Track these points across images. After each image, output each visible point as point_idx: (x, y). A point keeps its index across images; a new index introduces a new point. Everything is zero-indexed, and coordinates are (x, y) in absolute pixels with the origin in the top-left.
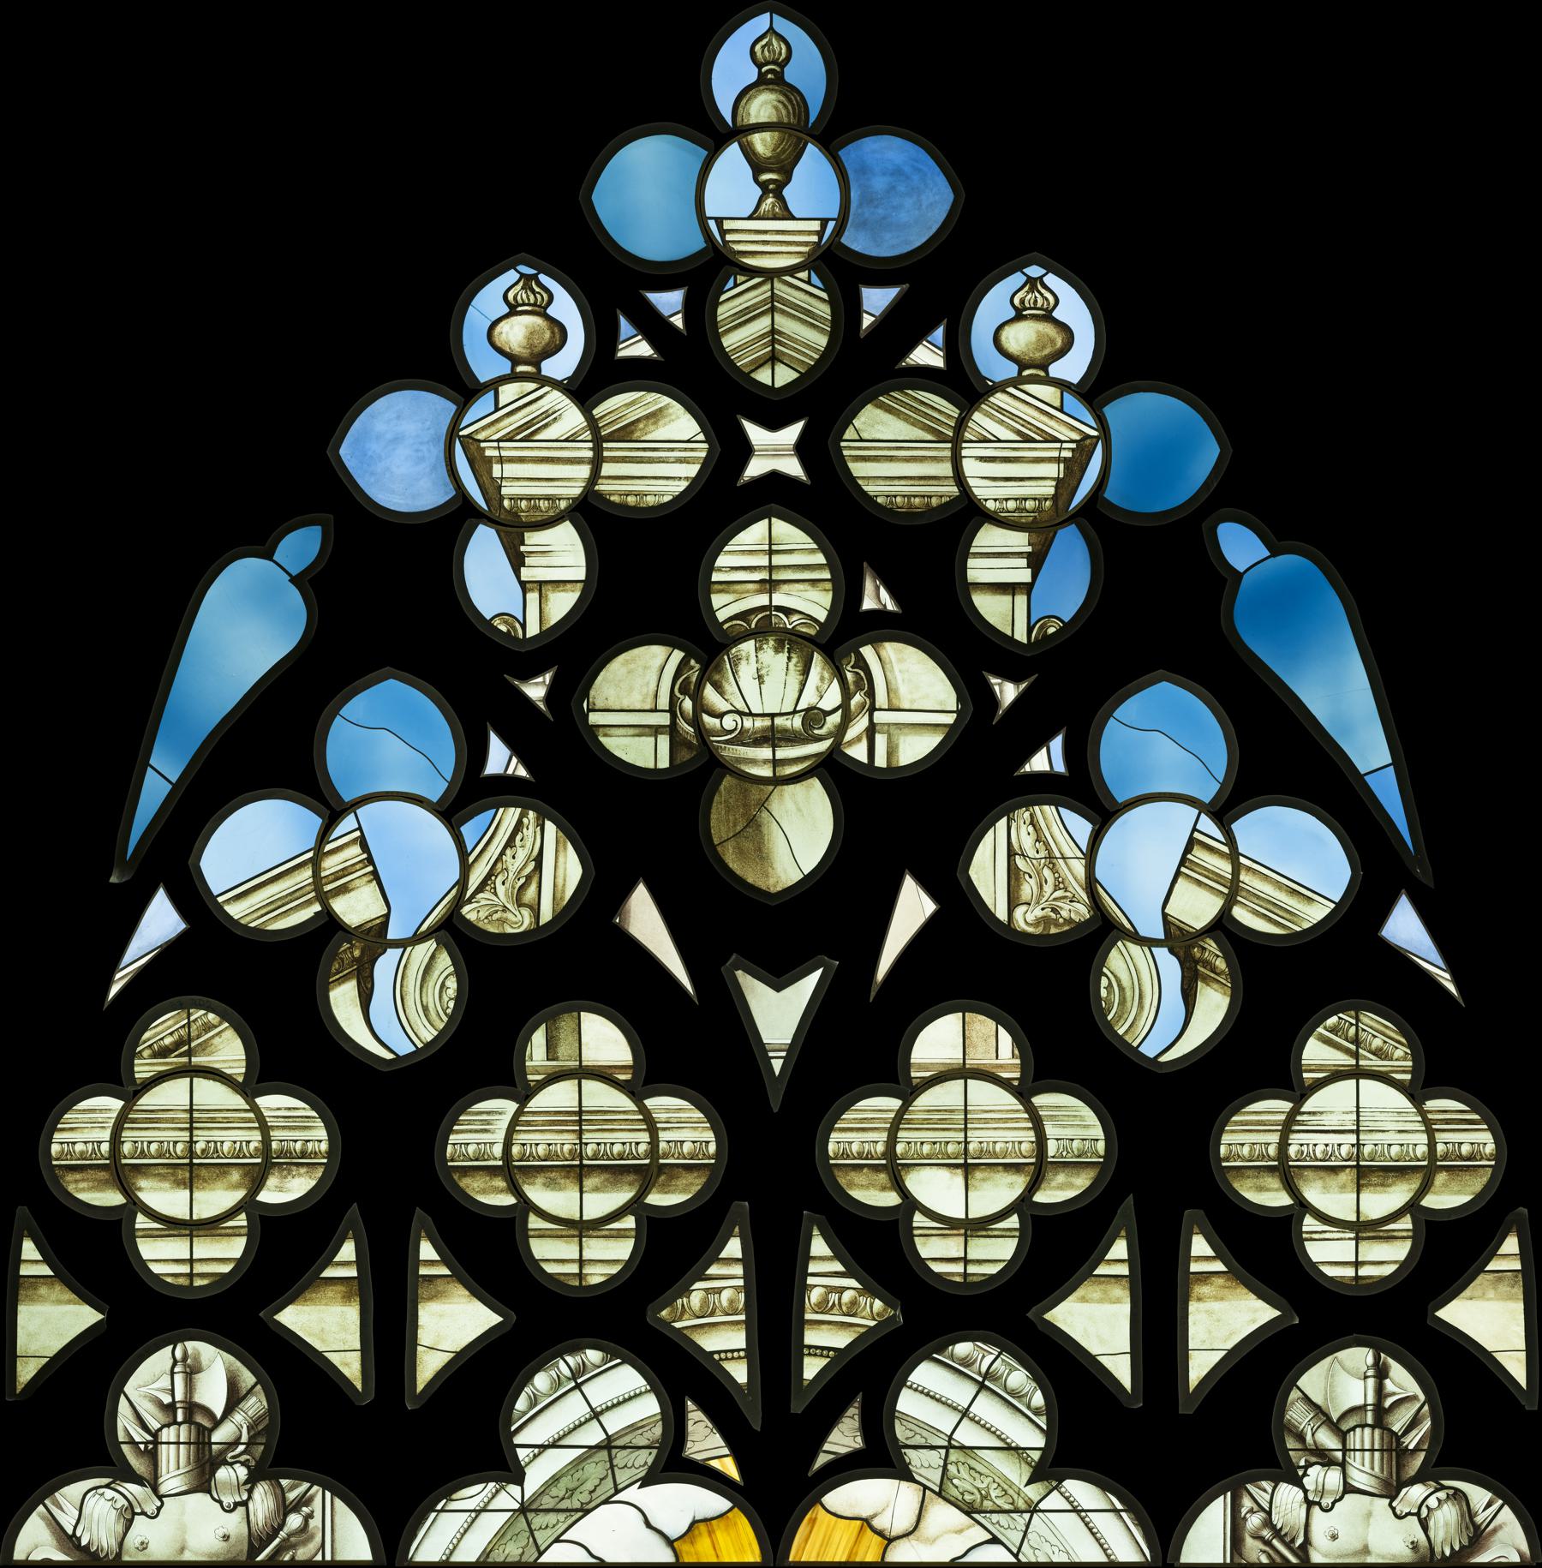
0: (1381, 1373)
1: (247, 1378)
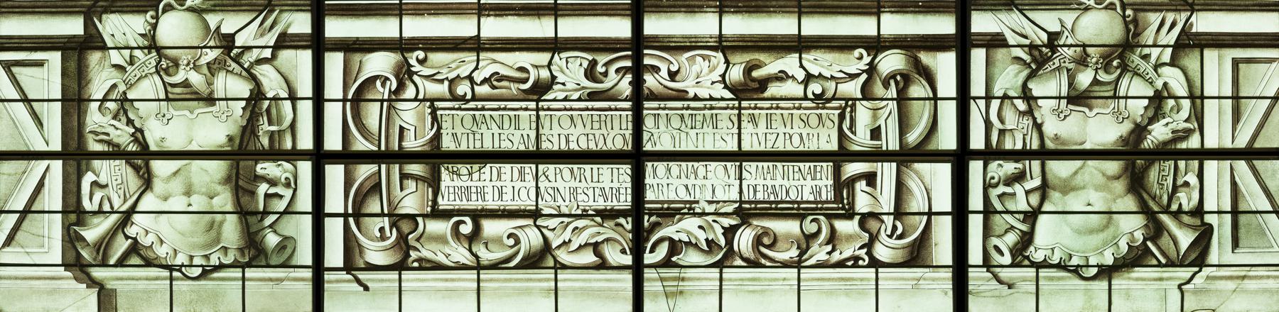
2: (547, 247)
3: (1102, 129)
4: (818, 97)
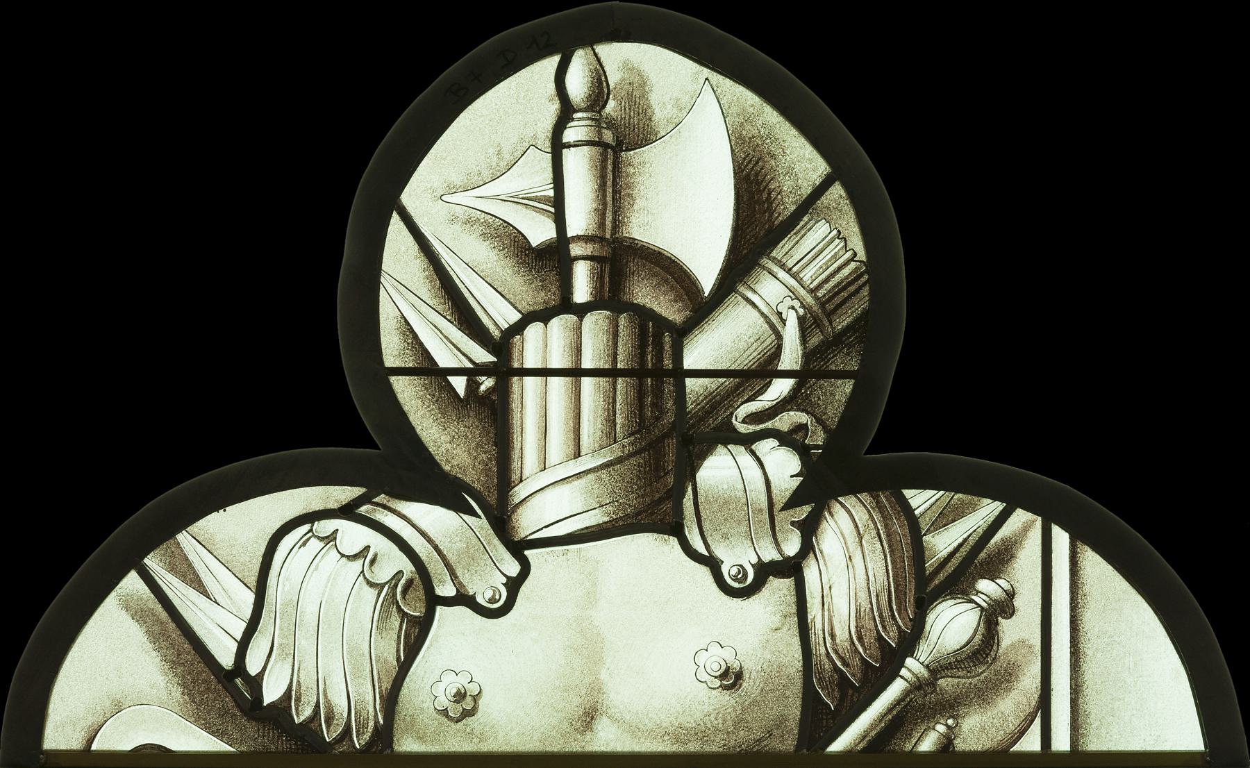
1: (800, 162)
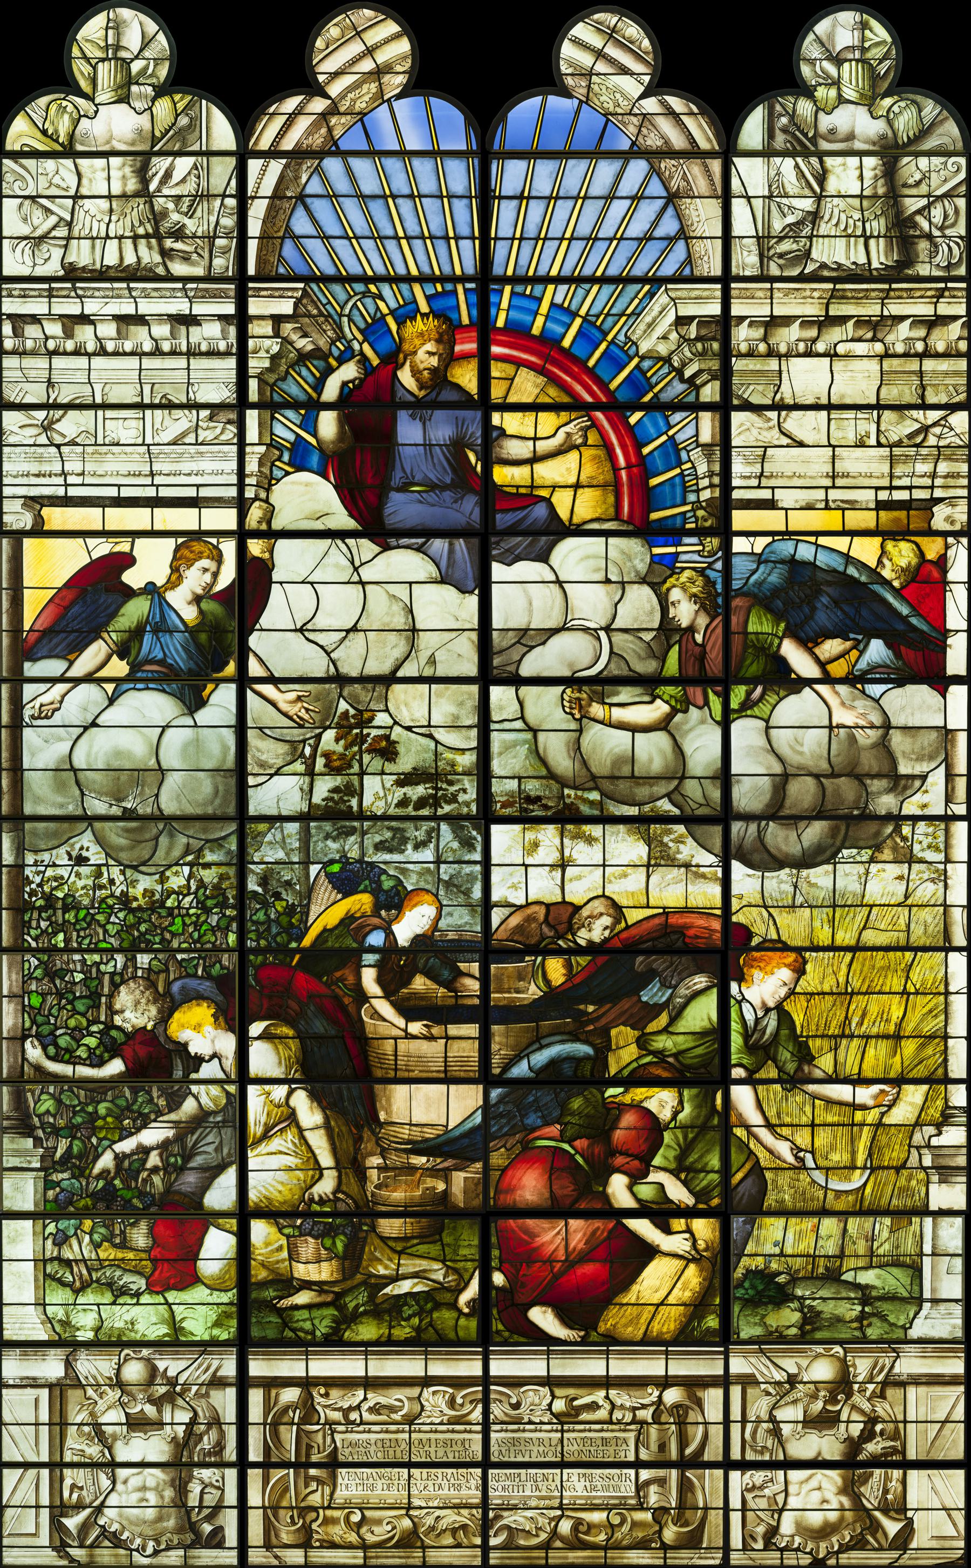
0: (864, 26)
2: (415, 1531)
3: (827, 1445)
4: (619, 1422)
